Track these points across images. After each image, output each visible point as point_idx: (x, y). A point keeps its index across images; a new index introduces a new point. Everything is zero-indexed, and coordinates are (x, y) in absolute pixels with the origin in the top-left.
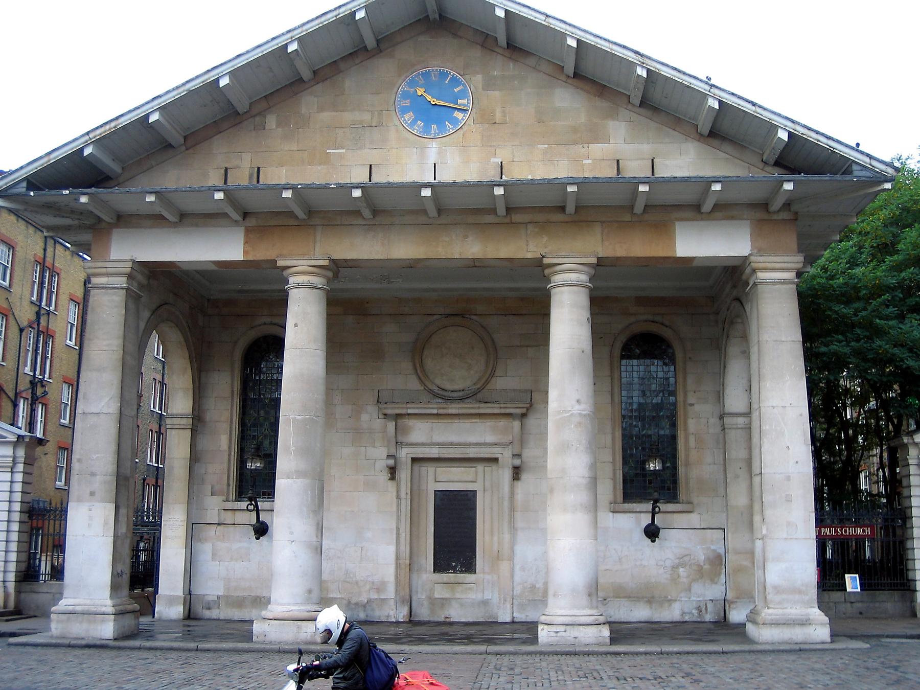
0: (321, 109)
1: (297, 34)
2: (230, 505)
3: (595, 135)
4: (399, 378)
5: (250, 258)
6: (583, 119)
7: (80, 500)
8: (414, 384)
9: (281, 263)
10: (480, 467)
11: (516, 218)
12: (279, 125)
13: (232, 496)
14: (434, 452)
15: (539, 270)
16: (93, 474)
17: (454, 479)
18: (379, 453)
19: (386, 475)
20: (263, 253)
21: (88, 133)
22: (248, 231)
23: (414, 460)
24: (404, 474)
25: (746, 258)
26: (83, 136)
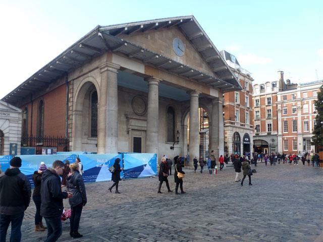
0: (159, 39)
1: (172, 19)
2: (90, 138)
3: (201, 66)
4: (129, 110)
5: (146, 74)
6: (199, 62)
7: (108, 136)
8: (132, 111)
9: (154, 77)
10: (142, 132)
11: (192, 80)
12: (151, 39)
13: (90, 136)
14: (136, 128)
15: (190, 92)
16: (112, 129)
17: (137, 135)
18: (125, 127)
19: (126, 133)
20: (149, 73)
21: (128, 23)
22: (145, 67)
23: (132, 129)
24: (130, 133)
25: (216, 98)
26: (126, 24)
